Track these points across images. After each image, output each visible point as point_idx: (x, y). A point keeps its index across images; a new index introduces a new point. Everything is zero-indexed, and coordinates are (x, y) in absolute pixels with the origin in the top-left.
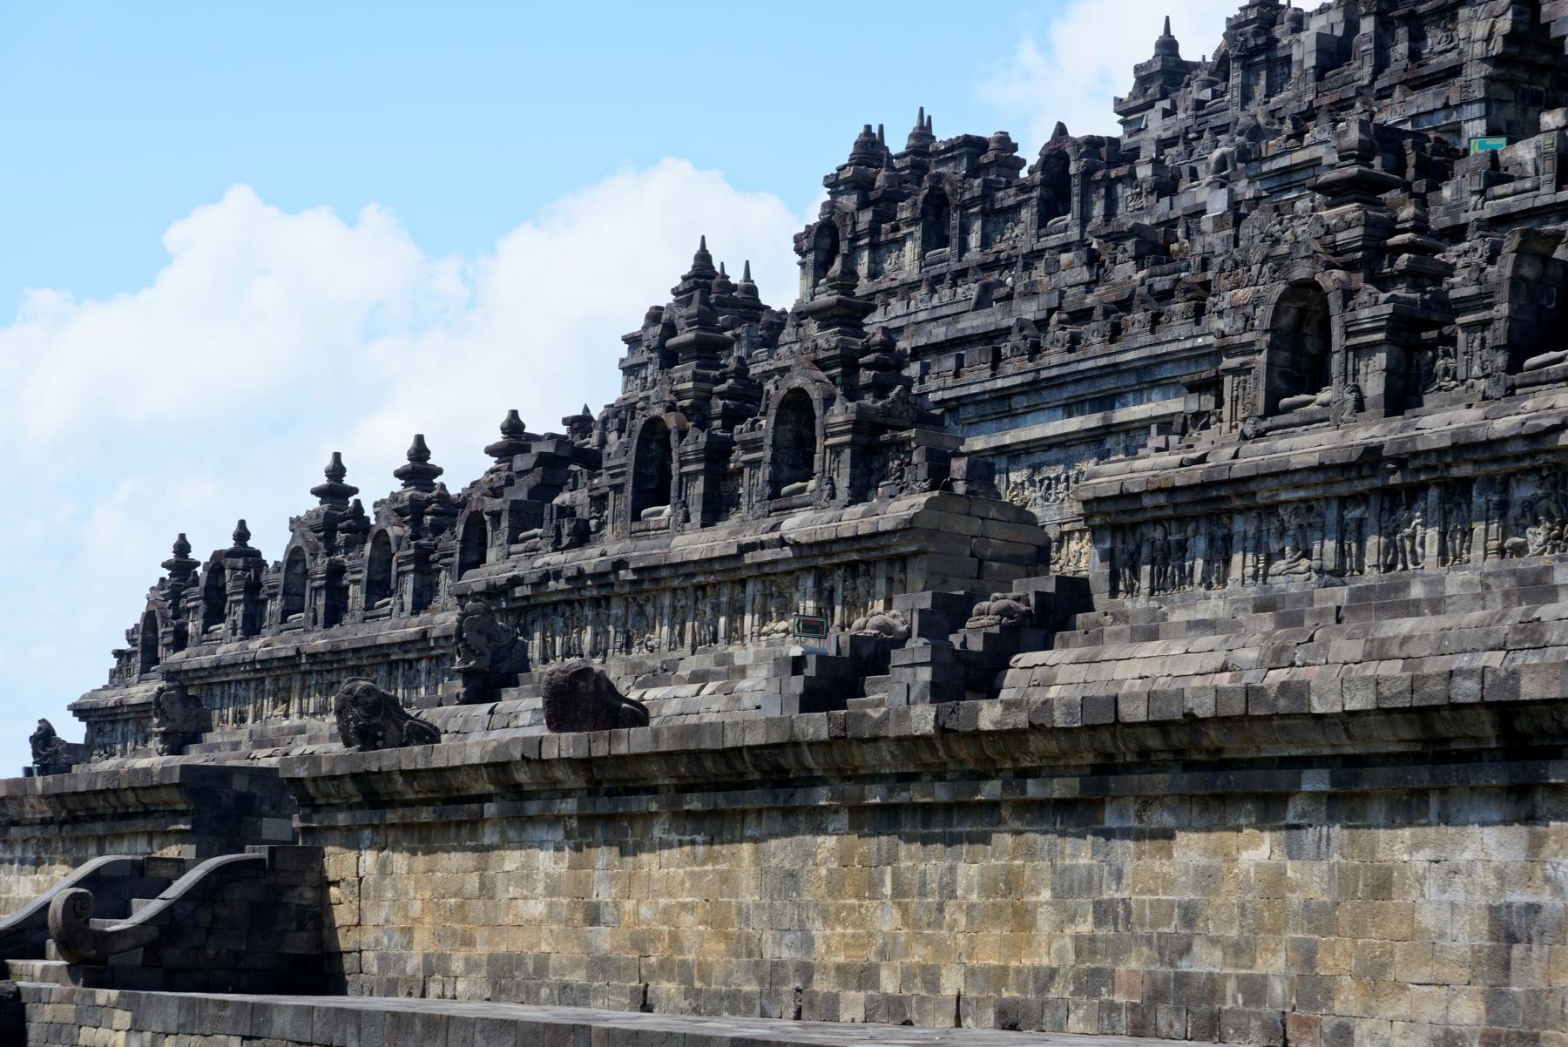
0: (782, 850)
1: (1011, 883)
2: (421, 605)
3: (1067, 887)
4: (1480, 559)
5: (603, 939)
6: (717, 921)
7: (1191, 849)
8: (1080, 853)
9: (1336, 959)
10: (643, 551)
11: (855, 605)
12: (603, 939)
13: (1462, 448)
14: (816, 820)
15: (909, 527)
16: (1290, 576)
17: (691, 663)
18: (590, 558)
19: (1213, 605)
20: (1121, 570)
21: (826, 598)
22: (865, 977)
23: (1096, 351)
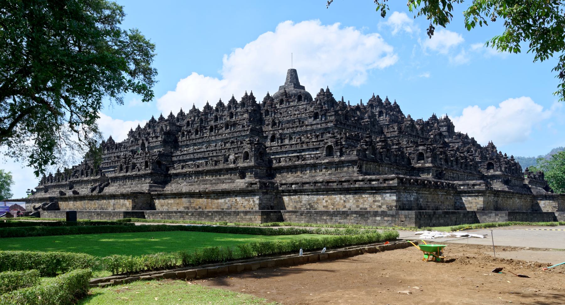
0: (84, 201)
1: (95, 203)
2: (66, 181)
3: (97, 203)
4: (130, 182)
5: (75, 207)
6: (81, 205)
7: (102, 201)
8: (98, 201)
9: (108, 206)
10: (82, 179)
11: (96, 183)
12: (75, 207)
13: (129, 175)
14: (86, 200)
15: (99, 178)
16: (121, 183)
17: (85, 187)
18: (78, 179)
19: (116, 184)
20: (112, 181)
21: (94, 183)
22: (88, 208)
23: (114, 165)
